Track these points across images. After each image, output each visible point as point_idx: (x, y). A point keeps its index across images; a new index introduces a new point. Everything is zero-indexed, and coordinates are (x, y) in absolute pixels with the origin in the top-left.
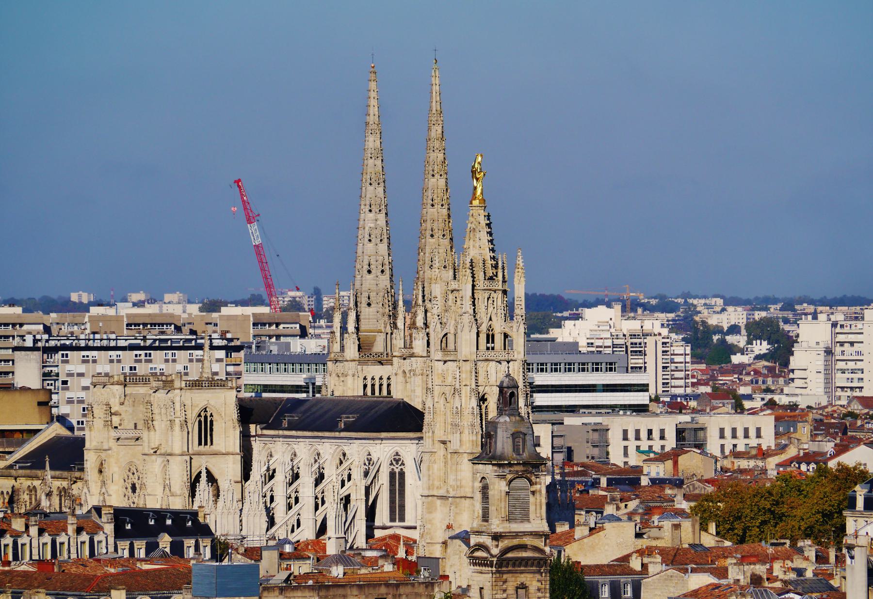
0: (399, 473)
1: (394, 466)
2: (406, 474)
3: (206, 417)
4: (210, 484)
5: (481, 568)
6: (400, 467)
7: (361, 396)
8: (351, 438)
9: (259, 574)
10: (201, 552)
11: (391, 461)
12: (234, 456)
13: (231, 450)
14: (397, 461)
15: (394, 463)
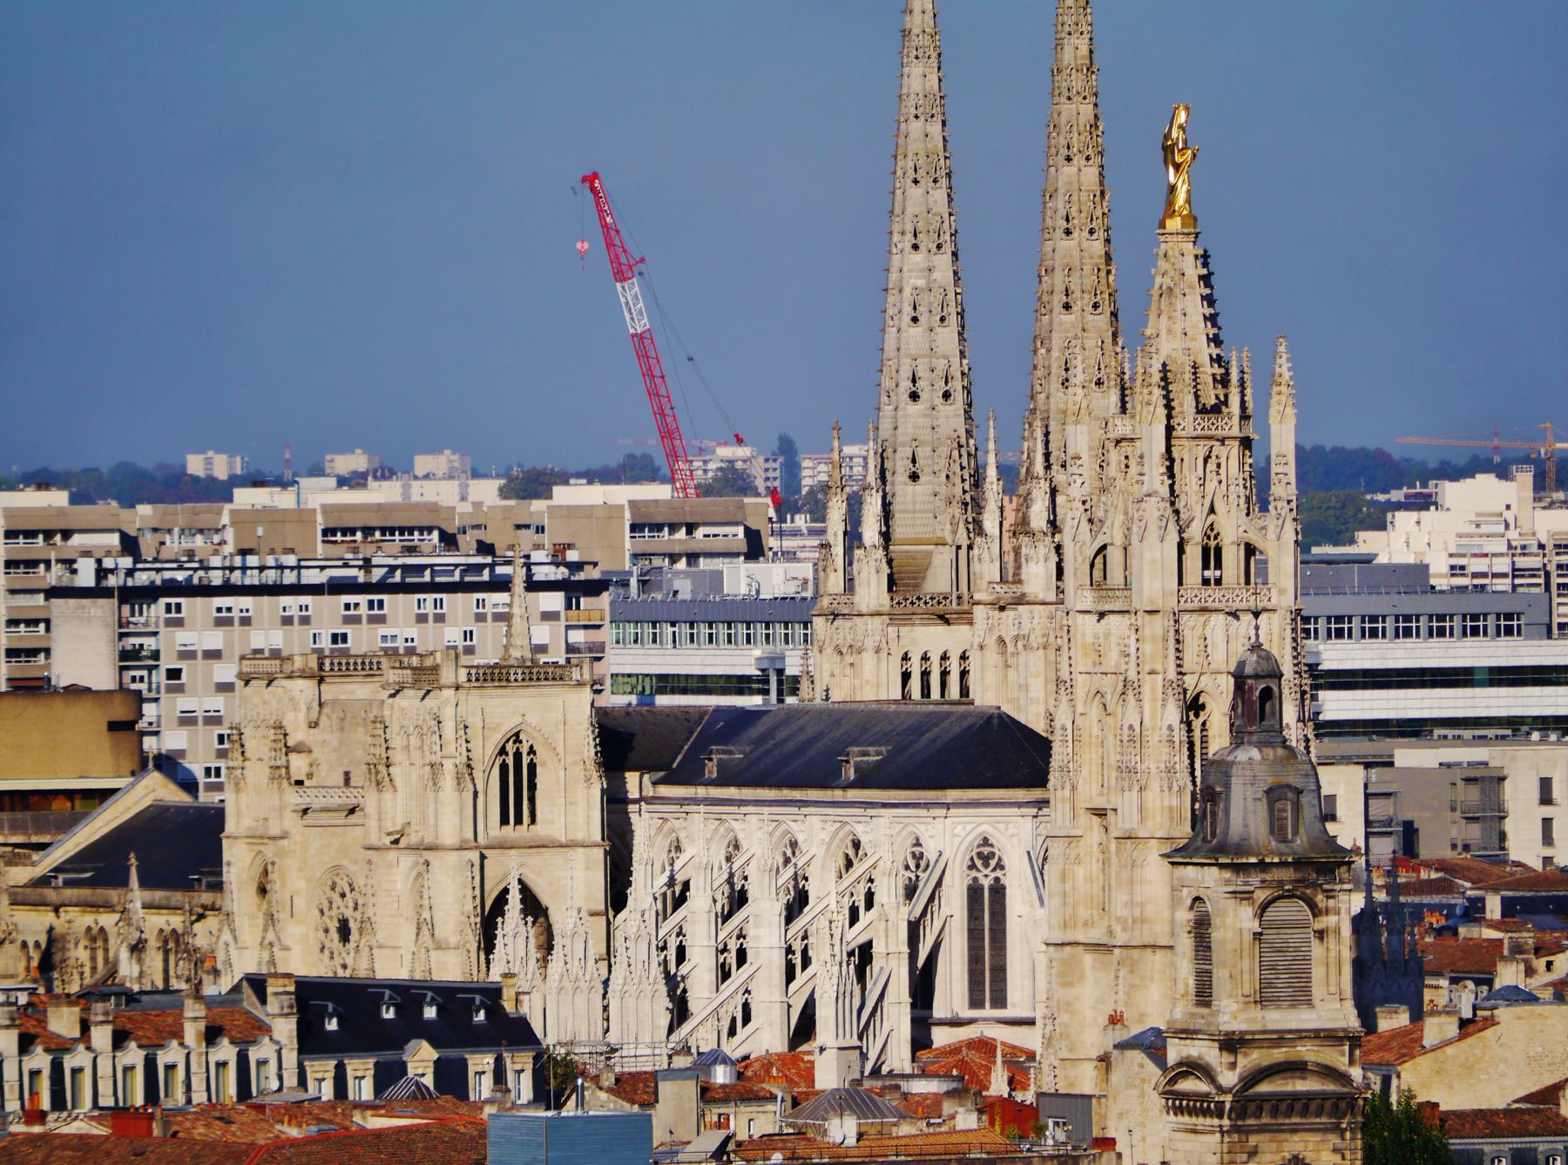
0: (991, 888)
1: (978, 870)
2: (1008, 892)
3: (518, 756)
4: (530, 919)
5: (1194, 1120)
6: (993, 875)
7: (895, 701)
8: (872, 805)
9: (651, 1138)
10: (510, 1085)
11: (972, 859)
12: (588, 849)
13: (580, 836)
14: (986, 859)
15: (979, 863)
